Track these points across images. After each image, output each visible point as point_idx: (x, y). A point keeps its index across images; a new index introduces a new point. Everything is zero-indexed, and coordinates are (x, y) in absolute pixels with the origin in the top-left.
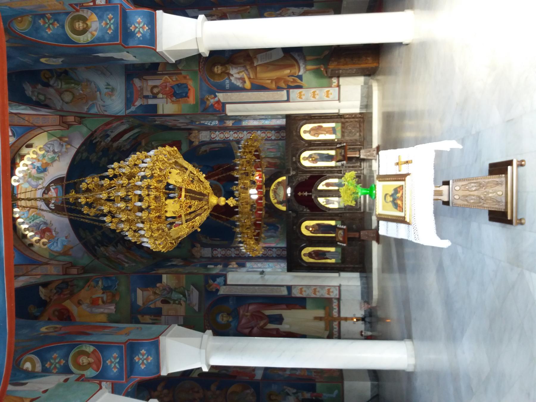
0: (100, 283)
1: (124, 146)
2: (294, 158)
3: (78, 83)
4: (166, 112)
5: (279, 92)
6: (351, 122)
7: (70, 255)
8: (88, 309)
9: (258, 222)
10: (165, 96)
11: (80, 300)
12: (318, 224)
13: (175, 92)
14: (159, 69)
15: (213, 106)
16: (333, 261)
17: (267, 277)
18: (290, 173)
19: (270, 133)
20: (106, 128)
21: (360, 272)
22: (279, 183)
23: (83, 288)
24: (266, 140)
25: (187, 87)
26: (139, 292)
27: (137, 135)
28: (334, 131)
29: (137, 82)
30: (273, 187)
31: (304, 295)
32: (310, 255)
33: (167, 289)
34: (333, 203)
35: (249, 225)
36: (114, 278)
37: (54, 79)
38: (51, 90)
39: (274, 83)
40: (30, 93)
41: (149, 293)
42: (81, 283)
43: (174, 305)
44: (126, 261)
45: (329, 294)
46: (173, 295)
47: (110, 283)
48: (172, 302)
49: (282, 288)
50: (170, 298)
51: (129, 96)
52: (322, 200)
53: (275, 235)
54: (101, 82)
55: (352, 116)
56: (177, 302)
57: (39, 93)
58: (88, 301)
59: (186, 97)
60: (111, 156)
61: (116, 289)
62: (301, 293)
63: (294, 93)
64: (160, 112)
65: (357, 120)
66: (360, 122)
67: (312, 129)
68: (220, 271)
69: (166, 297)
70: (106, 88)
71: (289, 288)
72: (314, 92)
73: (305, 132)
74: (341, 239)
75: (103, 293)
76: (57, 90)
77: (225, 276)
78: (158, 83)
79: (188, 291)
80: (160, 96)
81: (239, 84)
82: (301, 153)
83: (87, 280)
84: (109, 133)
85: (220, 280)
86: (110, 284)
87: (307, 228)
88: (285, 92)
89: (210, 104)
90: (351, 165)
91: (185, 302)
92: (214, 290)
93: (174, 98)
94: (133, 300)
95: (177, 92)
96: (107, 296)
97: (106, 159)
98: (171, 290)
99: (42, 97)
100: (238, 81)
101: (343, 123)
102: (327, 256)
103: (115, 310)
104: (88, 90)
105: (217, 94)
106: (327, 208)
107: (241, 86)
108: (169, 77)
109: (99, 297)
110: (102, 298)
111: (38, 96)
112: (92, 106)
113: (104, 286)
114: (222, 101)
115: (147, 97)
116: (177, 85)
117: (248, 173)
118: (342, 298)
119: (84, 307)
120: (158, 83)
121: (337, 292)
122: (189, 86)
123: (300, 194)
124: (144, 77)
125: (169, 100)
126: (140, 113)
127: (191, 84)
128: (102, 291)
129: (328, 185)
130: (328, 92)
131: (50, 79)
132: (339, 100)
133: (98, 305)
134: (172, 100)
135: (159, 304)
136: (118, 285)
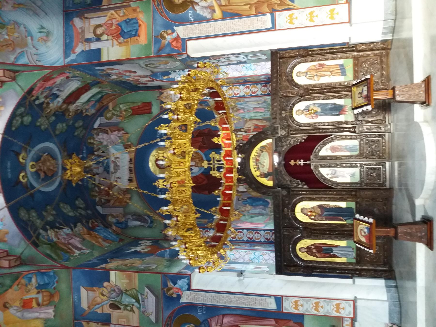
0: (34, 280)
1: (87, 110)
2: (283, 112)
4: (113, 57)
5: (259, 18)
6: (368, 56)
7: (5, 241)
8: (19, 314)
9: (225, 208)
10: (110, 37)
11: (7, 302)
12: (320, 206)
13: (122, 30)
14: (103, 5)
15: (170, 44)
16: (344, 260)
17: (247, 280)
18: (277, 133)
19: (255, 87)
20: (48, 84)
21: (386, 278)
22: (262, 147)
23: (11, 287)
24: (251, 96)
25: (138, 23)
26: (83, 292)
27: (99, 96)
28: (342, 70)
29: (78, 22)
30: (254, 153)
31: (301, 311)
32: (309, 250)
33: (117, 290)
34: (343, 176)
35: (192, 225)
36: (52, 274)
39: (254, 9)
41: (96, 294)
42: (8, 282)
43: (125, 312)
44: (80, 246)
45: (338, 311)
46: (123, 300)
47: (46, 280)
48: (122, 307)
49: (268, 299)
50: (120, 302)
51: (68, 41)
52: (326, 172)
53: (264, 212)
54: (32, 24)
55: (370, 47)
56: (129, 308)
58: (17, 304)
59: (135, 36)
60: (71, 122)
61: (55, 288)
62: (296, 308)
63: (282, 18)
64: (104, 58)
65: (376, 52)
66: (381, 56)
67: (310, 70)
68: (185, 268)
69: (115, 301)
70: (40, 32)
71: (279, 299)
72: (311, 13)
73: (299, 74)
74: (363, 240)
75: (38, 293)
77: (189, 277)
78: (101, 21)
79: (142, 294)
80: (105, 37)
81: (206, 14)
82: (294, 105)
83: (16, 277)
84: (55, 91)
85: (182, 283)
86: (47, 281)
87: (302, 210)
88: (269, 16)
89: (166, 42)
90: (370, 119)
91: (139, 308)
92: (175, 296)
93: (122, 38)
94: (76, 302)
95: (125, 31)
96: (43, 297)
97: (64, 125)
98: (121, 293)
100: (205, 10)
101: (355, 58)
102: (335, 252)
103: (53, 314)
104: (16, 35)
105: (175, 28)
106: (333, 183)
107: (209, 16)
108: (115, 12)
109: (33, 298)
110: (37, 299)
112: (22, 54)
113: (39, 284)
114: (182, 36)
115: (88, 41)
116: (125, 21)
117: (186, 126)
118: (359, 318)
119: (12, 311)
120: (101, 21)
121: (351, 309)
122: (139, 21)
123: (292, 163)
124: (86, 15)
125: (115, 42)
126: (81, 61)
127: (142, 18)
128: (36, 291)
129: (334, 149)
130: (333, 10)
132: (350, 21)
133: (32, 308)
134: (119, 41)
135: (107, 310)
136: (57, 282)
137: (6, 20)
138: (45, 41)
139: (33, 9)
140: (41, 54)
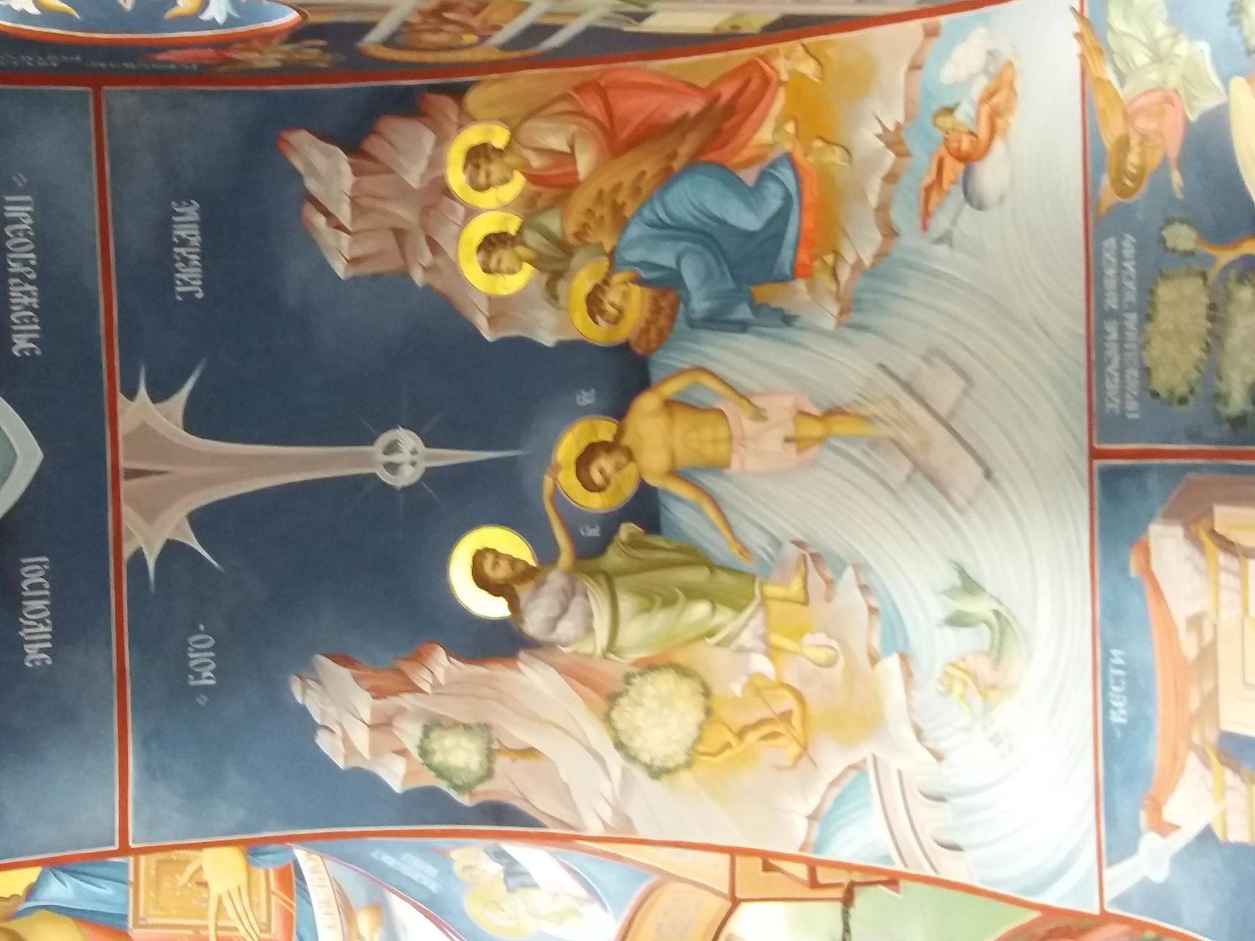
3: (734, 582)
37: (556, 579)
38: (533, 678)
40: (361, 738)
57: (433, 725)
70: (957, 621)
76: (578, 675)
99: (460, 753)
111: (424, 752)
131: (524, 591)
137: (756, 541)
138: (987, 689)
139: (909, 439)
140: (960, 793)
